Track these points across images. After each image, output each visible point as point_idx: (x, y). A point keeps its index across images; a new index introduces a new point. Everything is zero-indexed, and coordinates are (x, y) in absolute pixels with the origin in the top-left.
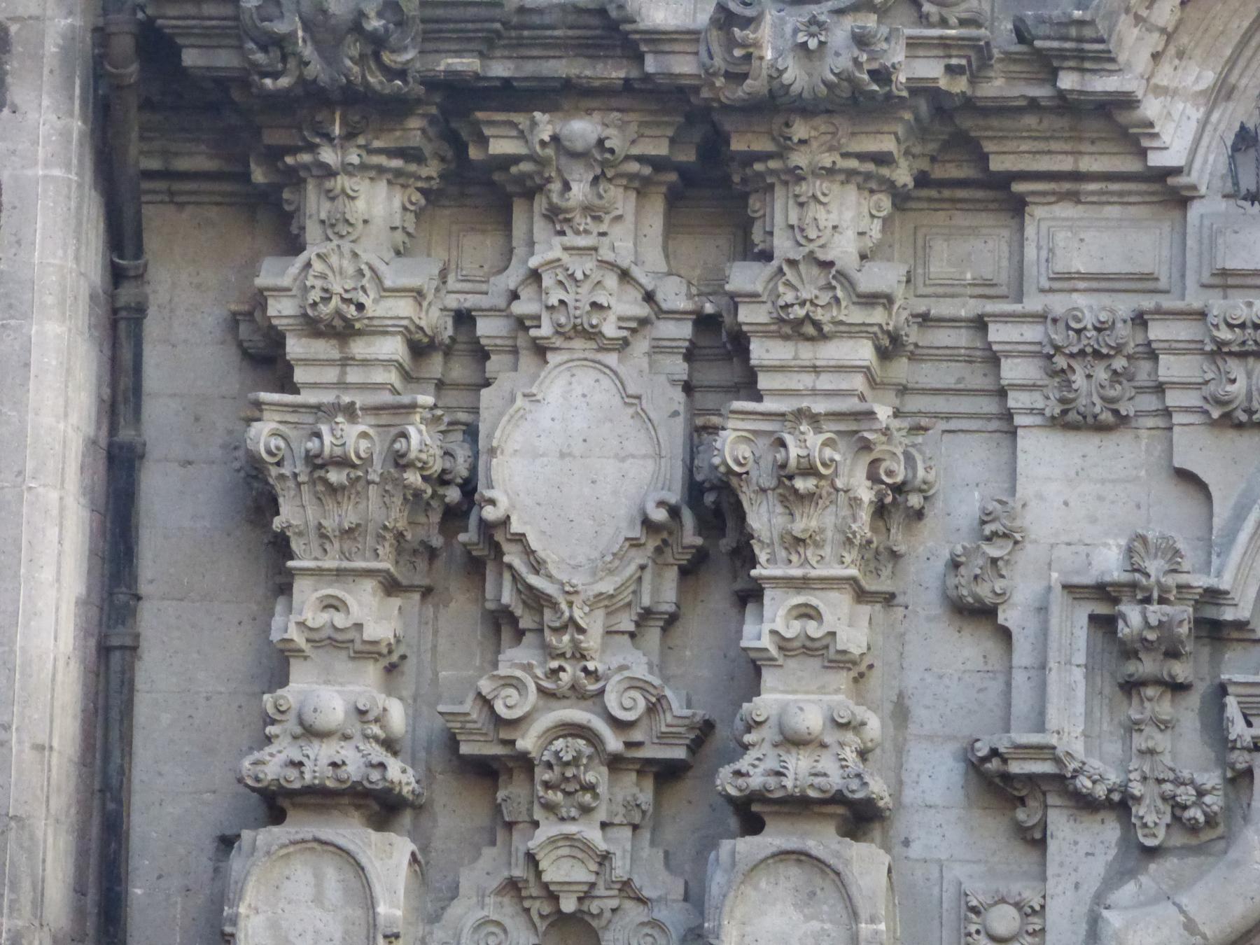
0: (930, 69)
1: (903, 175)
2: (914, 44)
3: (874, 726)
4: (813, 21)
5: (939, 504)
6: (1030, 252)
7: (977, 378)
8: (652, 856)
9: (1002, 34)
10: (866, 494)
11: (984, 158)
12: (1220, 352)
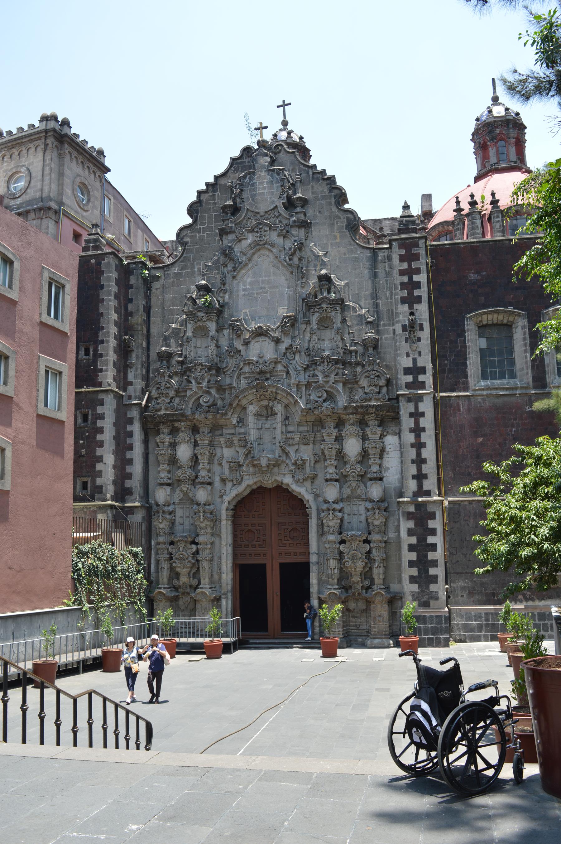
3: (210, 475)
8: (193, 487)
12: (239, 440)
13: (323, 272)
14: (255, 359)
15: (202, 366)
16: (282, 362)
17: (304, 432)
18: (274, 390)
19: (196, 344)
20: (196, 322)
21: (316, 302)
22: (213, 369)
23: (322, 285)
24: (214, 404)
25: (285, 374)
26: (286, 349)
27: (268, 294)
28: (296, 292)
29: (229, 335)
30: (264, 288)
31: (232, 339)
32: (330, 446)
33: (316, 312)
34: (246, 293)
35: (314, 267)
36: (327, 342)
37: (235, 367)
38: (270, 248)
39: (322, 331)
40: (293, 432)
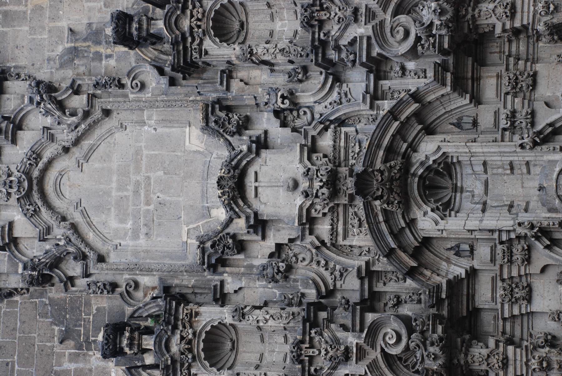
0: (440, 328)
1: (467, 337)
2: (434, 331)
4: (427, 356)
5: (551, 332)
6: (487, 307)
7: (518, 321)
9: (433, 311)
10: (547, 349)
11: (464, 317)
13: (109, 31)
14: (299, 200)
15: (302, 342)
16: (315, 133)
17: (499, 86)
18: (381, 153)
19: (248, 364)
20: (194, 358)
21: (175, 44)
22: (316, 316)
23: (139, 29)
24: (406, 321)
25: (344, 129)
26: (284, 125)
27: (151, 175)
28: (151, 104)
29: (237, 276)
30: (138, 183)
31: (251, 267)
32: (540, 5)
33: (201, 43)
34: (144, 230)
35: (101, 60)
36: (278, 26)
37: (318, 263)
38: (41, 165)
39: (250, 36)
40: (497, 114)
